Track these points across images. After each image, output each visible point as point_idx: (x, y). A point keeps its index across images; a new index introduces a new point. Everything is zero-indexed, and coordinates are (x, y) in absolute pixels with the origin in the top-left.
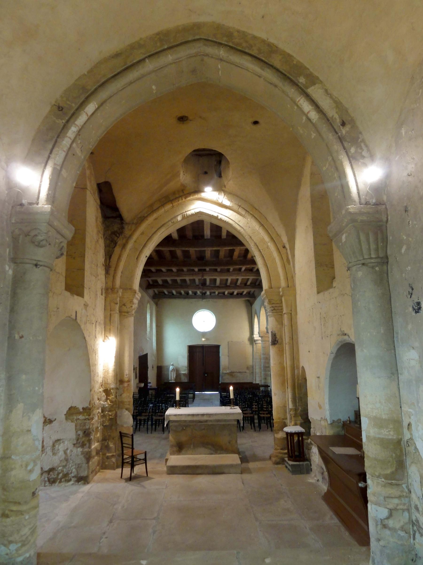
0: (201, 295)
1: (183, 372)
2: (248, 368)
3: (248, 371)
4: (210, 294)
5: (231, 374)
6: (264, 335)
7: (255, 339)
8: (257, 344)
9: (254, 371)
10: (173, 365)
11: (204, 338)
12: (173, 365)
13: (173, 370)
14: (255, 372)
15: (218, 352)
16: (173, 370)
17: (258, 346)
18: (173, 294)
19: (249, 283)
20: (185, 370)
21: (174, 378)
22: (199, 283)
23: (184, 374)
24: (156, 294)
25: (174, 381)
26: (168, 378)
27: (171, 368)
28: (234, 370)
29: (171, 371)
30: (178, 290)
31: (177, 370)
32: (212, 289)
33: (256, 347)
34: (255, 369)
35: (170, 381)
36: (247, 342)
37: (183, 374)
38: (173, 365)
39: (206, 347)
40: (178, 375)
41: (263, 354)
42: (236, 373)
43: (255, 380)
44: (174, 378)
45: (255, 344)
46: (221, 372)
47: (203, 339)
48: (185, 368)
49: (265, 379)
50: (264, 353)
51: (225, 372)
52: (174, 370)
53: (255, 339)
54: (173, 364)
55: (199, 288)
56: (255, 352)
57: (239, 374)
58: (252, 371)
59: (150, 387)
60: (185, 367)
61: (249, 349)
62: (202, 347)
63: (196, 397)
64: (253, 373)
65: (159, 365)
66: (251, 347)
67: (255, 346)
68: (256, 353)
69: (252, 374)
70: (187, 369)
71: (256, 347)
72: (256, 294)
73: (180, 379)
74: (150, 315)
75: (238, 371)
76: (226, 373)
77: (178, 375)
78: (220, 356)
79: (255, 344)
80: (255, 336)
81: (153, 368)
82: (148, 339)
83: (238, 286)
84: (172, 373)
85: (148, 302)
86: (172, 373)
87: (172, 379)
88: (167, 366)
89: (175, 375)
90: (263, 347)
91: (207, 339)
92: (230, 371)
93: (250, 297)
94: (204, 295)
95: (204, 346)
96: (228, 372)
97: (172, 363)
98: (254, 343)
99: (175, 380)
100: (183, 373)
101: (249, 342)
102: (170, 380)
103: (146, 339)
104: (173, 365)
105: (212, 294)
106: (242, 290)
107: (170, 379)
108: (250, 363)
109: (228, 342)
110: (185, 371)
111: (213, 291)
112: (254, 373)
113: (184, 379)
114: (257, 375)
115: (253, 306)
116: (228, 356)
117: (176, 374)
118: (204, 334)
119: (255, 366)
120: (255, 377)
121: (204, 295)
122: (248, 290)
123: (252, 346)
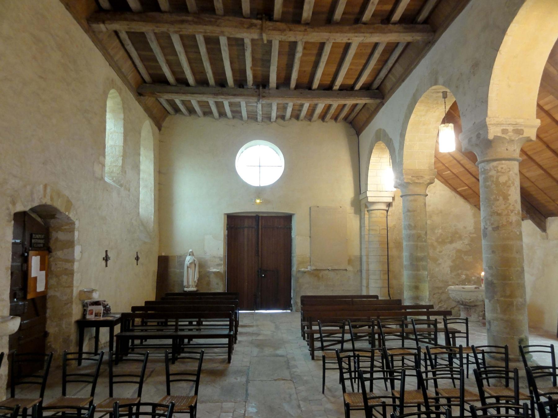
0: (255, 87)
1: (214, 268)
2: (350, 262)
3: (350, 268)
4: (277, 88)
5: (316, 273)
6: (414, 178)
7: (370, 200)
8: (371, 212)
9: (364, 267)
10: (193, 255)
11: (259, 197)
12: (192, 254)
13: (193, 263)
14: (368, 270)
15: (289, 229)
16: (193, 265)
17: (373, 216)
18: (188, 85)
19: (397, 16)
20: (219, 265)
21: (195, 282)
22: (251, 10)
23: (216, 273)
24: (144, 81)
25: (194, 289)
26: (183, 281)
27: (188, 259)
28: (320, 266)
29: (188, 267)
30: (189, 29)
31: (201, 265)
32: (290, 30)
33: (369, 217)
34: (368, 264)
35: (186, 289)
36: (349, 209)
37: (214, 273)
38: (192, 254)
39: (262, 217)
40: (203, 276)
41: (409, 227)
42: (327, 272)
43: (367, 287)
44: (195, 282)
45: (368, 211)
46: (294, 269)
47: (258, 201)
48: (218, 261)
49: (417, 288)
50: (413, 225)
51: (302, 270)
52: (195, 265)
53: (370, 200)
54: (192, 252)
55: (251, 26)
56: (367, 228)
57: (332, 275)
58: (359, 268)
59: (96, 315)
60: (220, 257)
61: (353, 222)
62: (257, 218)
63: (240, 329)
64: (361, 271)
65: (163, 254)
66: (358, 219)
67: (367, 216)
68: (369, 230)
69: (359, 273)
70: (222, 262)
71: (370, 217)
72: (388, 85)
73: (209, 283)
74: (123, 125)
75: (330, 268)
76: (305, 272)
77: (203, 276)
78: (293, 235)
79: (366, 212)
80: (369, 194)
81: (137, 259)
82: (107, 179)
83: (365, 24)
84: (191, 271)
85: (112, 85)
86: (191, 271)
87: (190, 283)
88: (180, 257)
89: (197, 276)
90: (408, 211)
91: (266, 202)
92: (314, 268)
93: (372, 97)
94: (261, 88)
95: (261, 215)
96: (309, 268)
97: (190, 250)
98: (366, 210)
99: (196, 286)
100: (215, 270)
101: (353, 208)
102: (184, 287)
103: (102, 179)
104: (193, 255)
105: (282, 89)
106: (375, 38)
107: (185, 283)
108: (355, 251)
109: (310, 208)
110: (220, 268)
111: (291, 37)
112: (364, 272)
113: (217, 284)
114: (372, 277)
115: (360, 137)
116: (310, 237)
117: (199, 272)
118: (259, 191)
119: (367, 256)
120: (368, 279)
121: (261, 88)
122: (392, 37)
123: (358, 216)
